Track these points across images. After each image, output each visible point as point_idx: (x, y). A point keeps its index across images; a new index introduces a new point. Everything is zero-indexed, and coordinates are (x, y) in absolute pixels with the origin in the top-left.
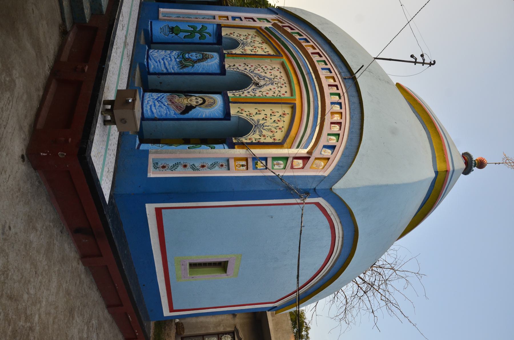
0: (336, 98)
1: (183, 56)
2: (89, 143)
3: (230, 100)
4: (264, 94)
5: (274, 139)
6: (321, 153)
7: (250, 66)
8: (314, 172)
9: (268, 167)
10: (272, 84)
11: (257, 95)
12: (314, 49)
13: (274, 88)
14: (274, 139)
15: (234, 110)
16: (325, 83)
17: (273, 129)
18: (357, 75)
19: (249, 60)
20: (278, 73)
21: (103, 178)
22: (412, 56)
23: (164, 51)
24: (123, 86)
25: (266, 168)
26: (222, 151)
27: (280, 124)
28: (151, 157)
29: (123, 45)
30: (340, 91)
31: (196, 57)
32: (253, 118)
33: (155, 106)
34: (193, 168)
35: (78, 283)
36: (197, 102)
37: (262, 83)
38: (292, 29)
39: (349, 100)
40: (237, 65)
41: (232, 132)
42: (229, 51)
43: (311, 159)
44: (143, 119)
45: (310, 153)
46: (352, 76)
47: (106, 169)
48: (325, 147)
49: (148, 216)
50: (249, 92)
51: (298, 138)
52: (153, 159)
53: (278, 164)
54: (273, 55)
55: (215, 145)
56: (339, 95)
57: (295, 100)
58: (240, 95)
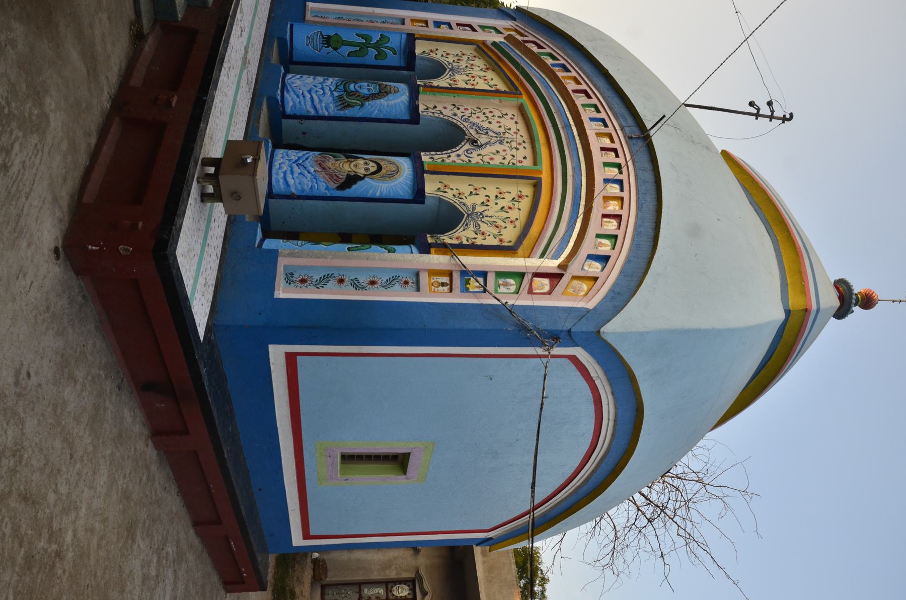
0: (613, 172)
1: (344, 87)
2: (174, 232)
3: (426, 168)
4: (486, 159)
5: (501, 241)
6: (582, 269)
7: (462, 109)
8: (569, 300)
9: (488, 288)
10: (501, 142)
11: (473, 161)
12: (578, 83)
13: (504, 151)
14: (501, 241)
15: (431, 186)
16: (595, 145)
17: (500, 223)
18: (652, 132)
19: (461, 99)
20: (511, 124)
21: (196, 295)
22: (752, 104)
23: (312, 77)
24: (238, 134)
25: (485, 291)
26: (407, 258)
27: (513, 214)
28: (282, 262)
29: (240, 63)
30: (621, 160)
31: (369, 90)
32: (465, 201)
33: (292, 173)
34: (356, 285)
35: (145, 478)
36: (367, 169)
37: (483, 140)
38: (540, 47)
39: (636, 175)
40: (440, 107)
41: (426, 225)
42: (427, 81)
43: (564, 278)
44: (270, 195)
45: (563, 267)
46: (643, 133)
47: (201, 280)
48: (590, 257)
49: (272, 367)
50: (459, 155)
51: (542, 240)
52: (285, 267)
53: (506, 284)
54: (505, 92)
55: (395, 247)
56: (619, 166)
57: (541, 172)
58: (443, 161)
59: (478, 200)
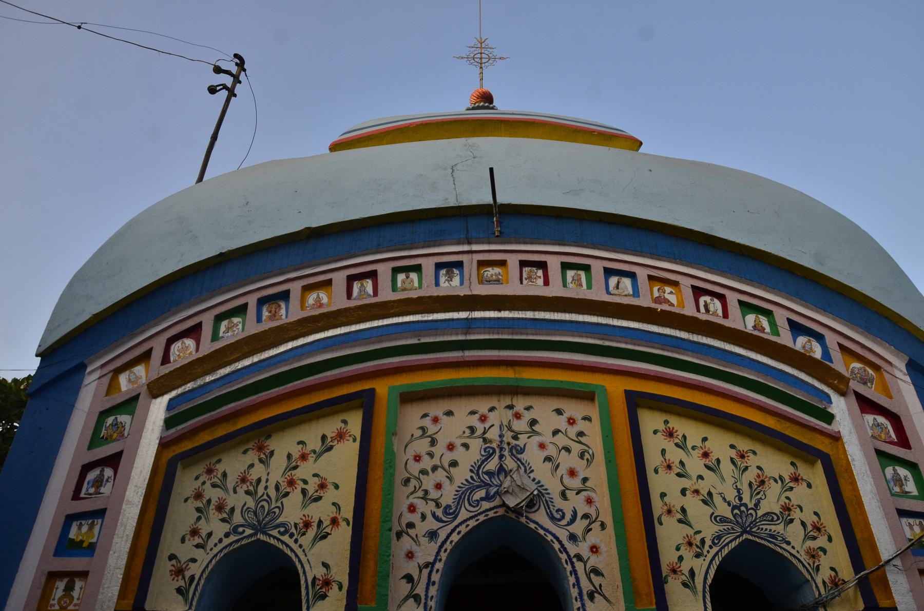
7: (415, 518)
18: (502, 199)
59: (698, 511)
